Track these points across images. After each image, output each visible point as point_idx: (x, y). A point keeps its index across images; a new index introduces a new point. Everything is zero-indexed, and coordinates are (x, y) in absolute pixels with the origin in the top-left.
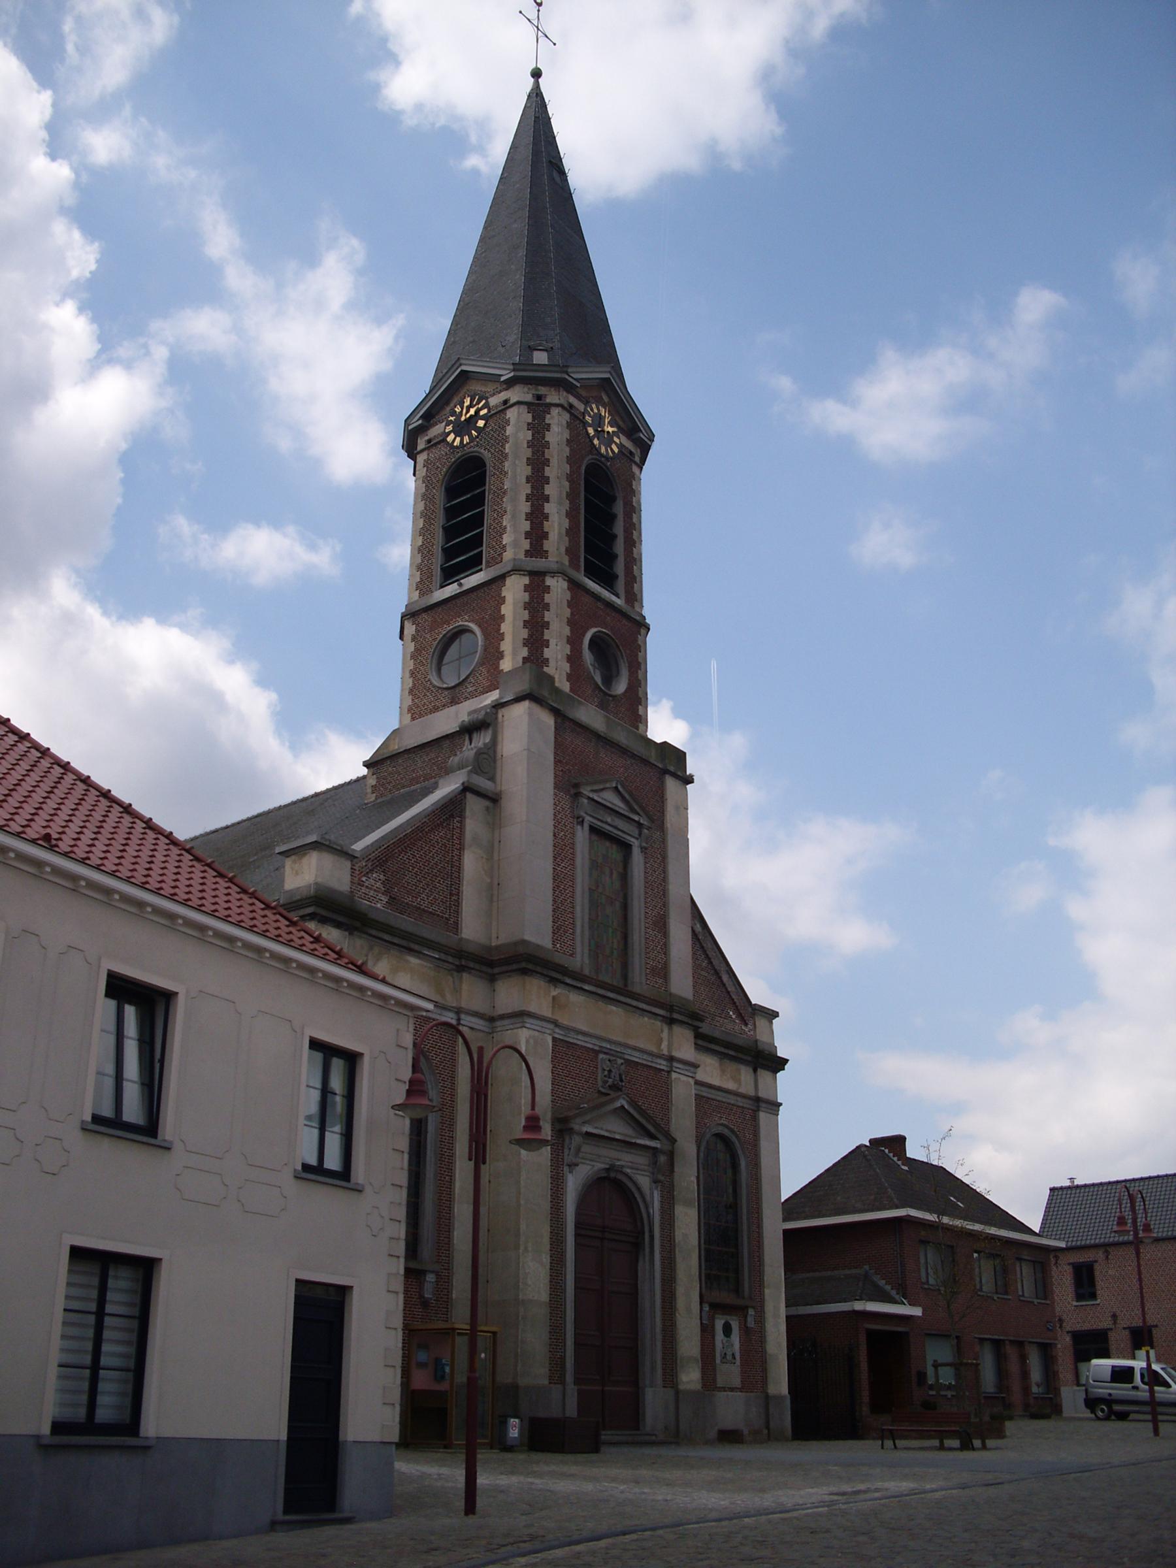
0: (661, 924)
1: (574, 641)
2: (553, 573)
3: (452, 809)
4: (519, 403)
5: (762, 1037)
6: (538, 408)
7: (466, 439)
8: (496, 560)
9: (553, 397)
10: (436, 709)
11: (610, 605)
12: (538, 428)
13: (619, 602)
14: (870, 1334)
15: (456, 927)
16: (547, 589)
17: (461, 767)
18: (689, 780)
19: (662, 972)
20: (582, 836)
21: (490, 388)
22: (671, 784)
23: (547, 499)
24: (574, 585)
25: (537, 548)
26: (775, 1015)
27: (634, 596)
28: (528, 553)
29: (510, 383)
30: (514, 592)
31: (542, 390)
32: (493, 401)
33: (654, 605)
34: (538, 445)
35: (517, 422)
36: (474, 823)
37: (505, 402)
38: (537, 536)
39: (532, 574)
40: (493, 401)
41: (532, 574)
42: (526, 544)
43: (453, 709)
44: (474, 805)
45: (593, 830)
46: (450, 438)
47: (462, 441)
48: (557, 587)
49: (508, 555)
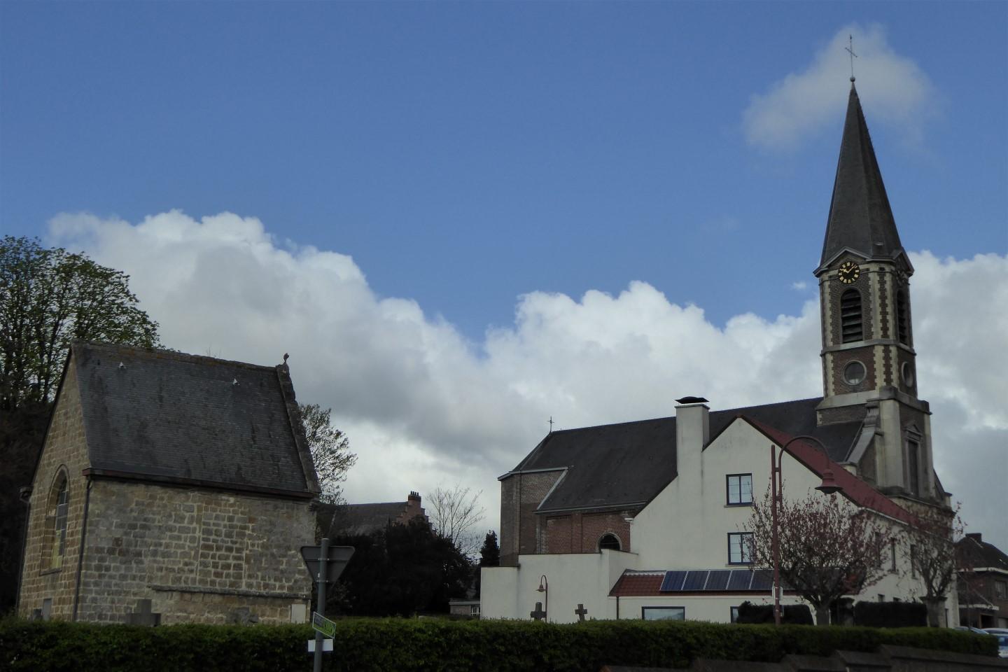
0: (926, 472)
1: (899, 371)
2: (892, 345)
3: (872, 441)
4: (874, 272)
5: (948, 505)
6: (881, 273)
7: (849, 281)
8: (869, 336)
9: (887, 269)
10: (846, 393)
11: (907, 351)
12: (882, 282)
13: (907, 348)
14: (983, 617)
15: (875, 481)
16: (890, 351)
17: (870, 423)
18: (930, 414)
19: (927, 489)
20: (907, 444)
21: (859, 261)
22: (926, 416)
23: (887, 313)
24: (899, 348)
25: (885, 335)
26: (950, 495)
27: (911, 344)
28: (882, 336)
29: (869, 262)
30: (879, 353)
31: (883, 265)
32: (861, 267)
33: (917, 346)
34: (882, 290)
35: (874, 279)
36: (877, 446)
37: (868, 270)
38: (885, 329)
39: (885, 346)
40: (861, 267)
41: (885, 346)
42: (881, 333)
43: (855, 394)
44: (878, 437)
45: (910, 442)
46: (842, 278)
47: (847, 281)
48: (893, 349)
49: (874, 337)
